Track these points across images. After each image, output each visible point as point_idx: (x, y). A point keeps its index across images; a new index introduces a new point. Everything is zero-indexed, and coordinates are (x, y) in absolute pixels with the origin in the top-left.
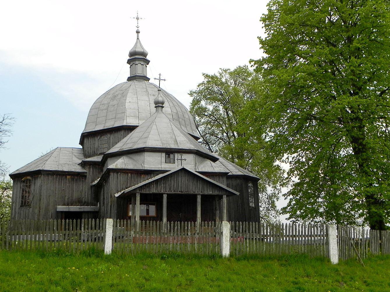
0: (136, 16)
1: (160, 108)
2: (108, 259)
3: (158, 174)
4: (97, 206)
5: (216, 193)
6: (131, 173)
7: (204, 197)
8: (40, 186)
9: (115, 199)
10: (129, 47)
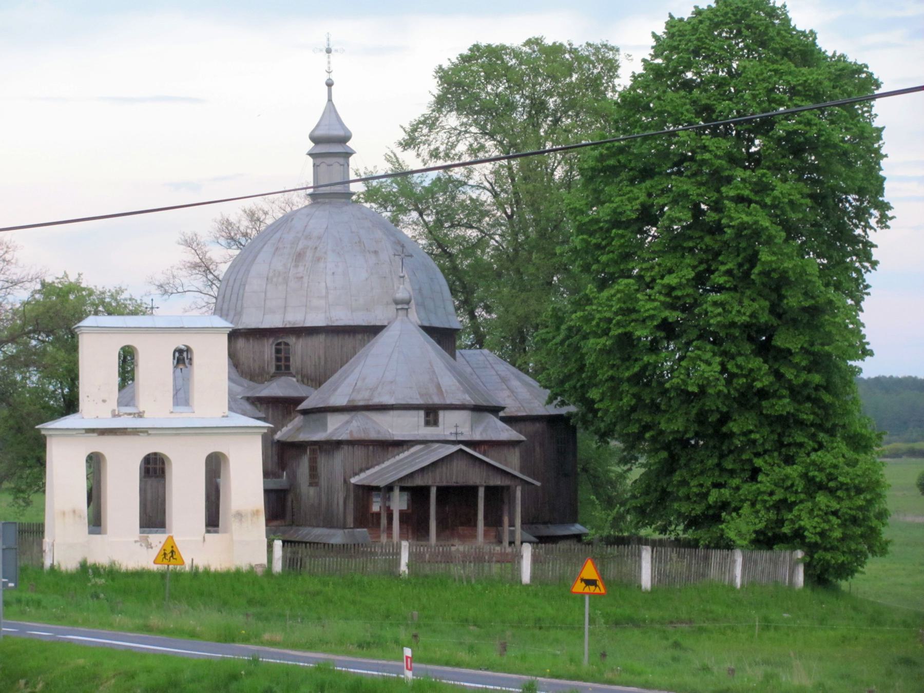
0: (324, 47)
2: (407, 582)
3: (412, 446)
5: (506, 482)
6: (374, 446)
7: (488, 489)
9: (352, 488)
10: (310, 121)
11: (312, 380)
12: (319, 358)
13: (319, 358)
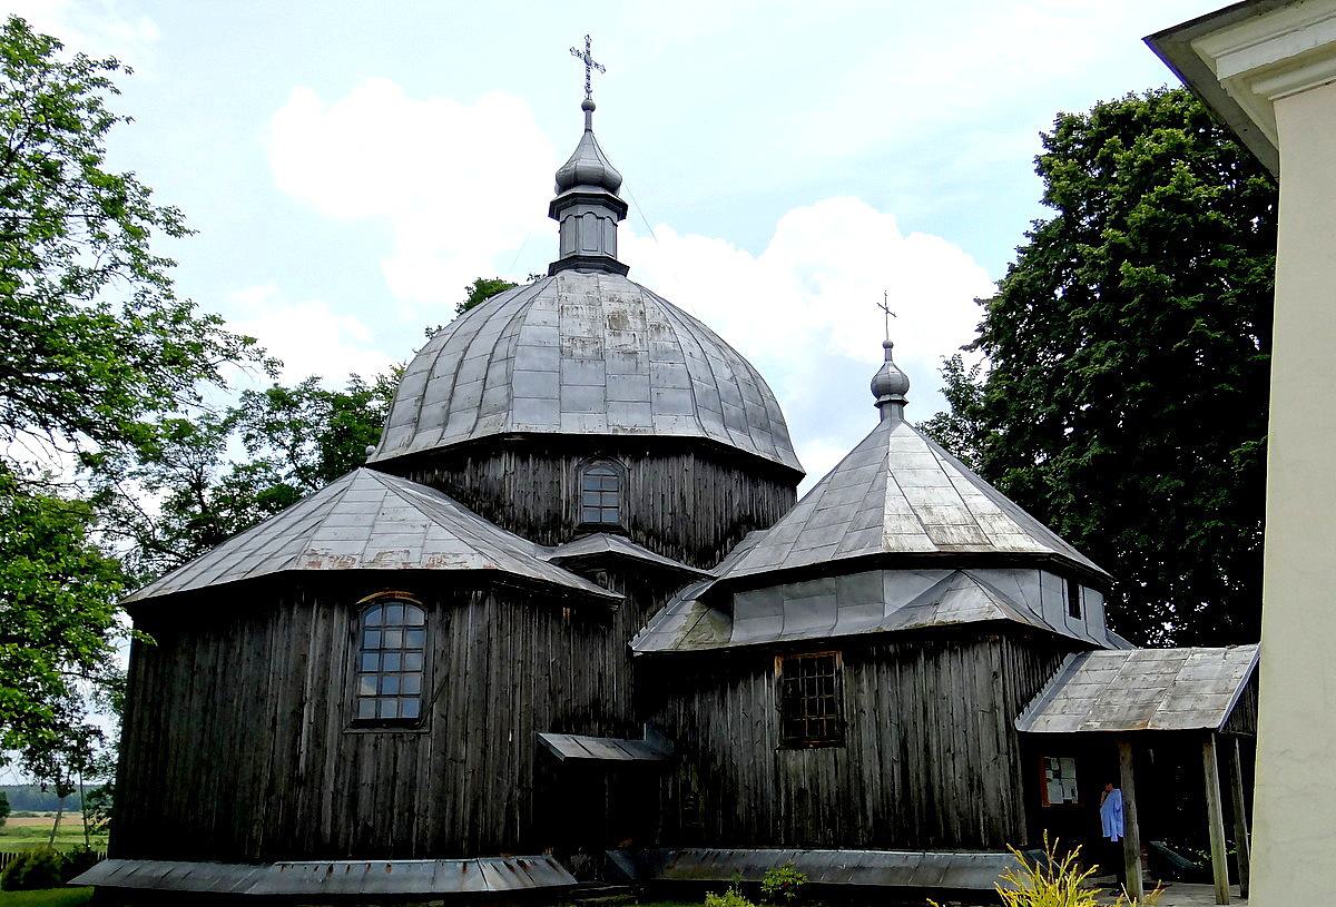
1: (895, 407)
4: (642, 739)
8: (479, 642)
11: (666, 544)
12: (683, 498)
13: (683, 498)
